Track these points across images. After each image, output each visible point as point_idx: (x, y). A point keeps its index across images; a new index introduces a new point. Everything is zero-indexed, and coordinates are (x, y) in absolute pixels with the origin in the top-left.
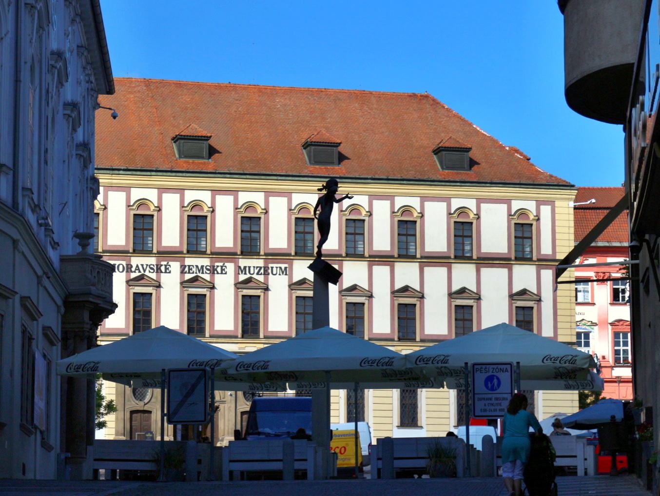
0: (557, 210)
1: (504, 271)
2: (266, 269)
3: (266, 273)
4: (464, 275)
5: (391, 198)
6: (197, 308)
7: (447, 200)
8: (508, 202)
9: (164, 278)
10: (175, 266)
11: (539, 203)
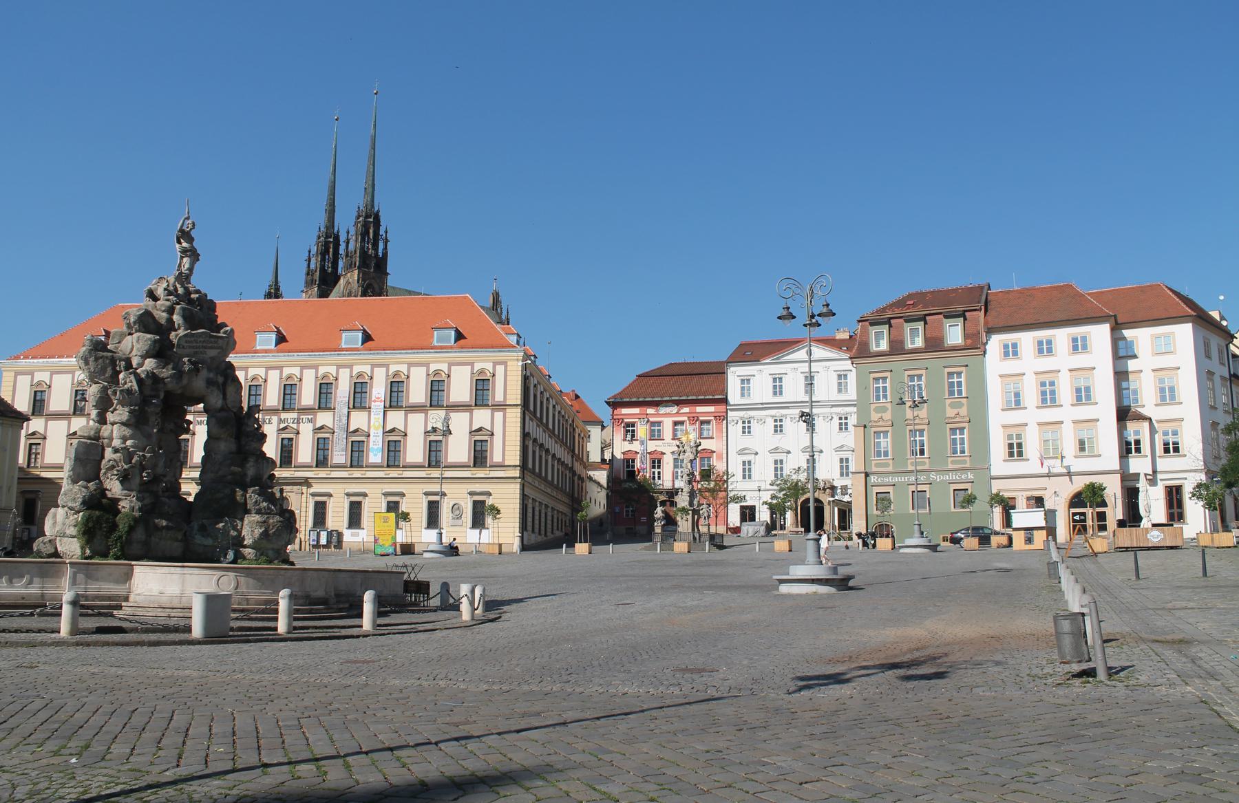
2: (298, 419)
3: (298, 423)
4: (436, 418)
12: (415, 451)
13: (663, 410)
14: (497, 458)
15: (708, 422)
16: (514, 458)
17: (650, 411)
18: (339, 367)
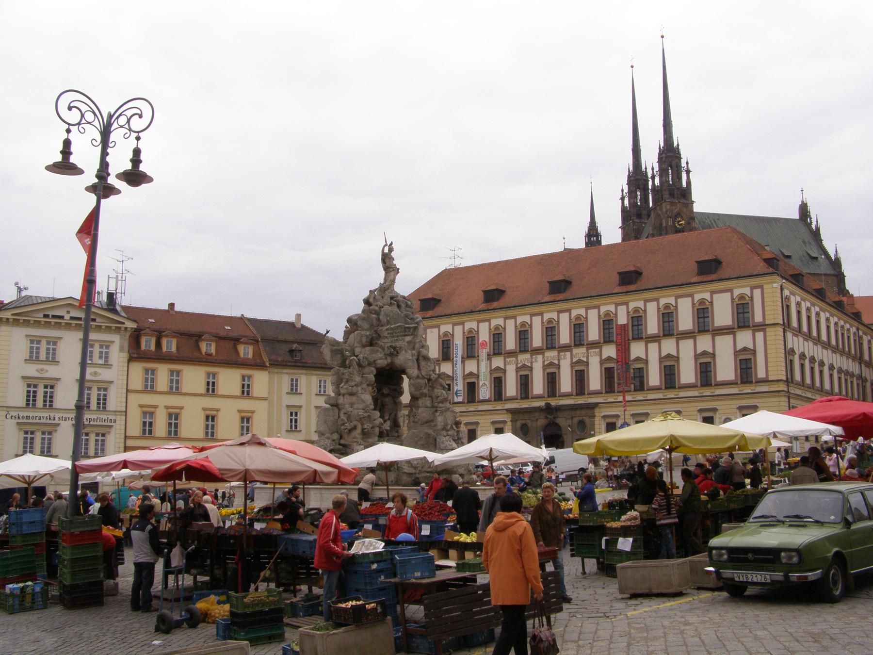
0: (765, 291)
1: (731, 337)
4: (704, 343)
5: (657, 300)
6: (552, 380)
7: (691, 296)
8: (731, 291)
9: (534, 365)
10: (540, 357)
11: (752, 288)
12: (687, 373)
14: (761, 374)
16: (778, 372)
18: (617, 305)
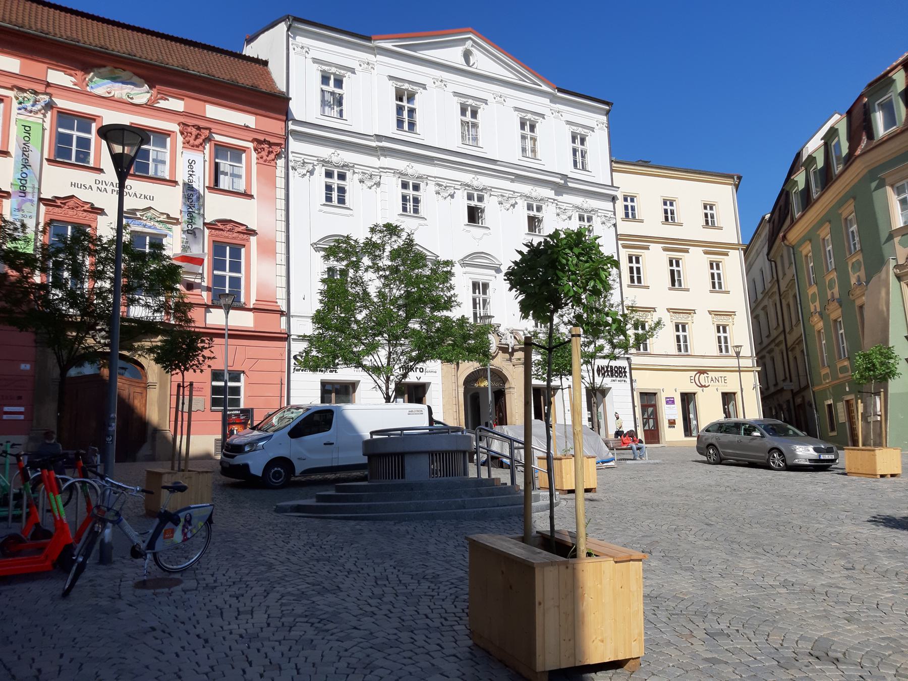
13: (102, 87)
15: (236, 153)
17: (57, 77)
